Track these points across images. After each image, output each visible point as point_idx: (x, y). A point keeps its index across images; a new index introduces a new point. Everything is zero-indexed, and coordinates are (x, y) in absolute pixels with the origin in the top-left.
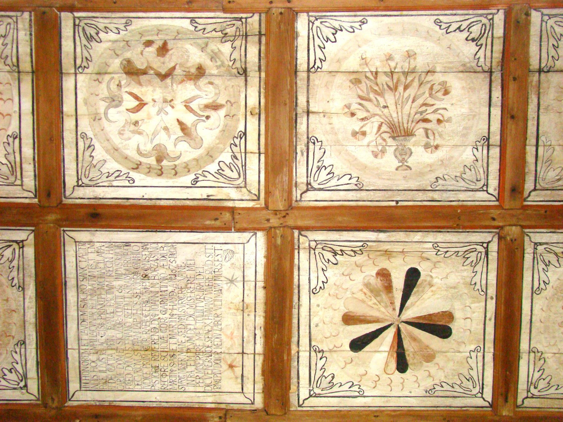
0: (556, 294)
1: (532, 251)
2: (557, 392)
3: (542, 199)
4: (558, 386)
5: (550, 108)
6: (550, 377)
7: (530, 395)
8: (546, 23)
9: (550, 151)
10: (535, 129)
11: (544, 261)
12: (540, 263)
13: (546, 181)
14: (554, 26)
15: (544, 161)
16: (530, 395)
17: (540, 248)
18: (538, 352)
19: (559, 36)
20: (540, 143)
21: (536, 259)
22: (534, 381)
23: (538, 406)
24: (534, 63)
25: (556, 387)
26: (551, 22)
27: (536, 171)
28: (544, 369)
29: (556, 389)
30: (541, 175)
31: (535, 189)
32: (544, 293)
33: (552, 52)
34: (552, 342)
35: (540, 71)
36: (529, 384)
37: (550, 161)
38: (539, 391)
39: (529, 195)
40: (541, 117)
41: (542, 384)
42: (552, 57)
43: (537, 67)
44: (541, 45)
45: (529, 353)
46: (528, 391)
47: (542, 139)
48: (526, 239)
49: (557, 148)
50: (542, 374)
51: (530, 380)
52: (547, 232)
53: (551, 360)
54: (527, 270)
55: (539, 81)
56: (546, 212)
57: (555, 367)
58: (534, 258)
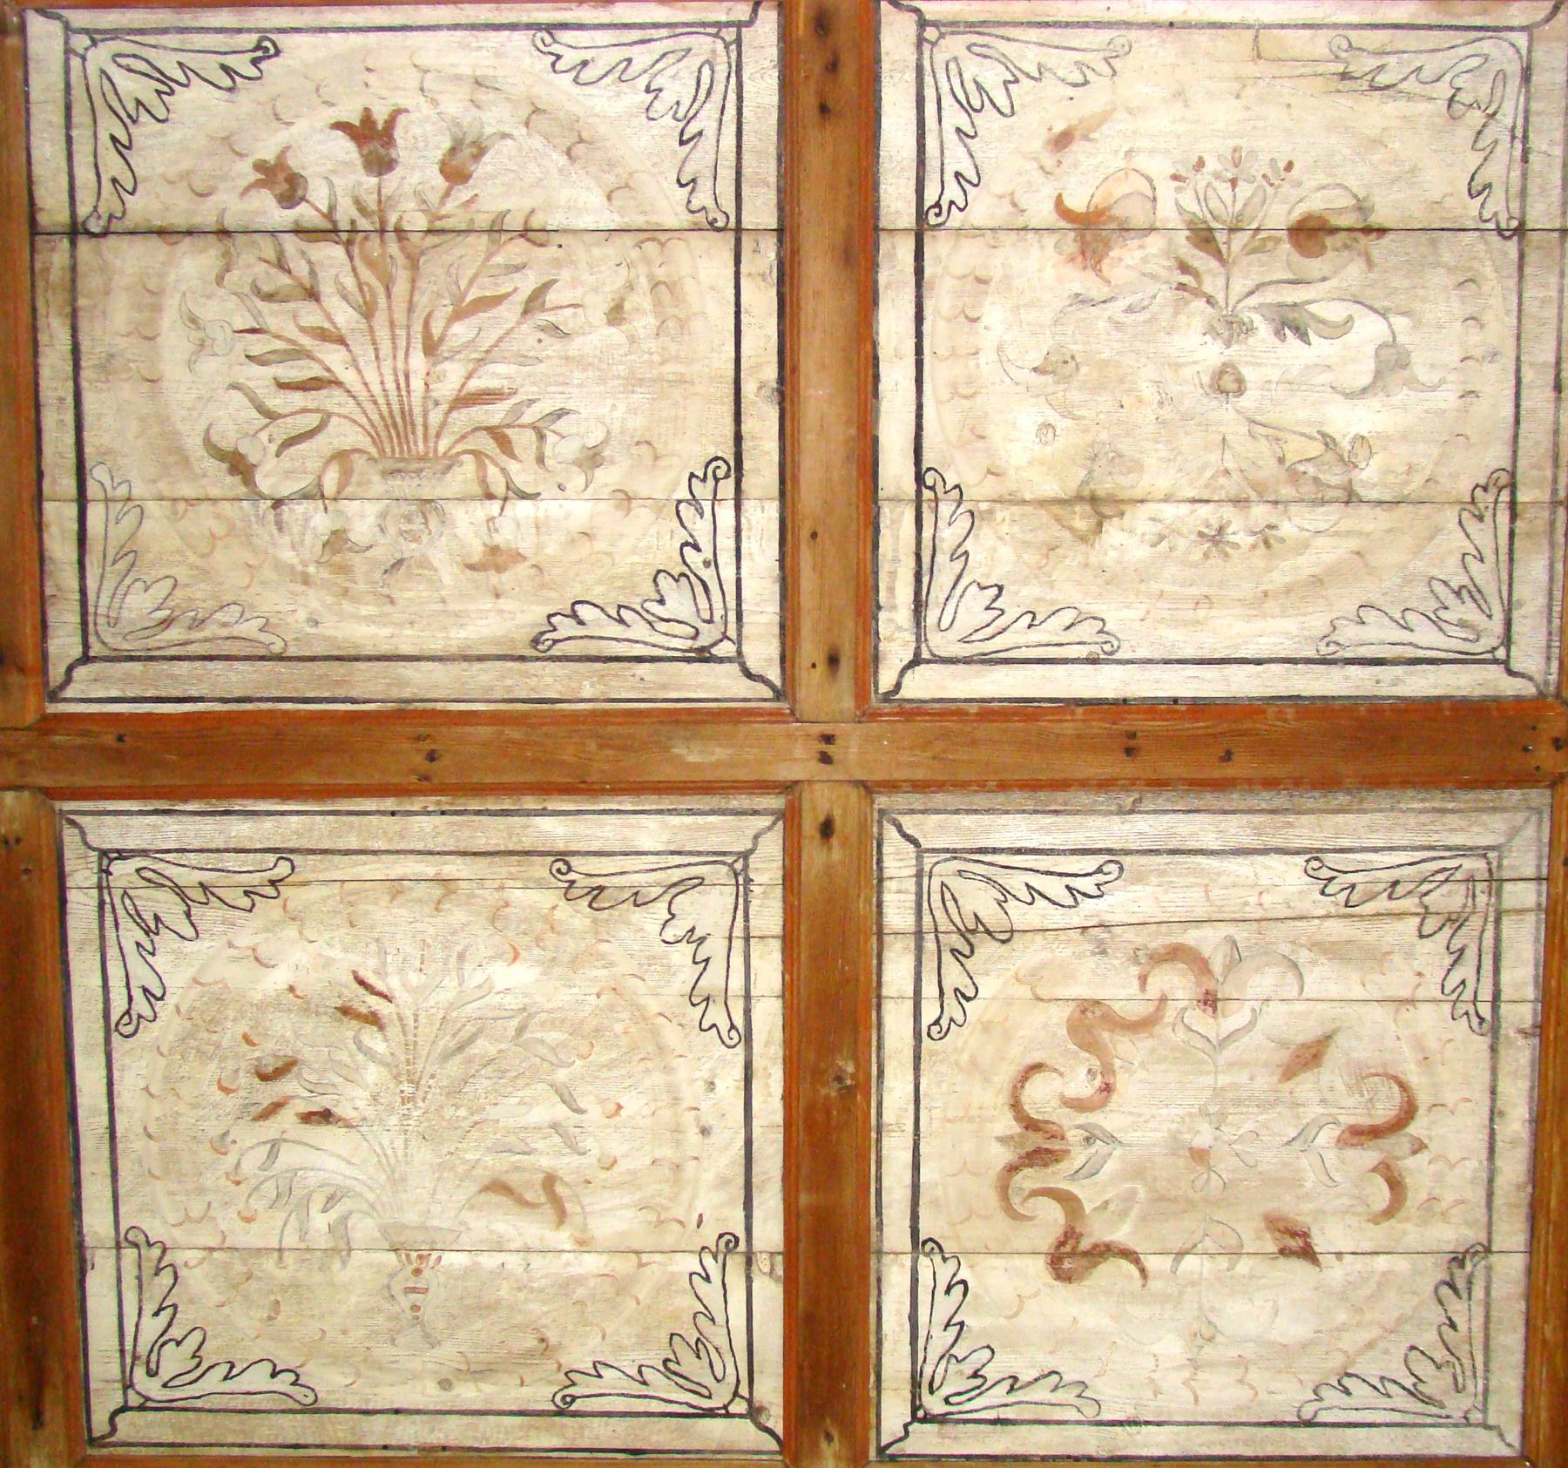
0: (191, 1035)
1: (95, 880)
2: (229, 1386)
3: (114, 693)
4: (232, 1366)
5: (117, 363)
6: (197, 1336)
7: (134, 1400)
8: (84, 59)
9: (129, 521)
10: (70, 439)
11: (137, 917)
12: (126, 922)
13: (124, 627)
14: (113, 71)
15: (110, 559)
16: (134, 1400)
17: (123, 871)
18: (149, 1245)
19: (131, 107)
20: (93, 490)
21: (108, 907)
22: (143, 1350)
23: (169, 1438)
24: (53, 207)
25: (224, 1368)
26: (100, 57)
27: (83, 591)
28: (175, 1306)
29: (226, 1378)
30: (102, 603)
31: (86, 659)
32: (149, 1033)
33: (112, 164)
34: (197, 1209)
35: (75, 231)
36: (129, 1360)
37: (130, 555)
38: (165, 1385)
39: (68, 679)
40: (88, 398)
41: (173, 1361)
42: (114, 181)
43: (63, 217)
44: (69, 140)
45: (118, 1247)
46: (128, 1385)
47: (98, 475)
48: (70, 837)
49: (151, 506)
50: (170, 1325)
51: (129, 1346)
52: (141, 813)
53: (197, 1272)
54: (81, 949)
55: (73, 269)
56: (120, 738)
57: (217, 1298)
58: (101, 904)
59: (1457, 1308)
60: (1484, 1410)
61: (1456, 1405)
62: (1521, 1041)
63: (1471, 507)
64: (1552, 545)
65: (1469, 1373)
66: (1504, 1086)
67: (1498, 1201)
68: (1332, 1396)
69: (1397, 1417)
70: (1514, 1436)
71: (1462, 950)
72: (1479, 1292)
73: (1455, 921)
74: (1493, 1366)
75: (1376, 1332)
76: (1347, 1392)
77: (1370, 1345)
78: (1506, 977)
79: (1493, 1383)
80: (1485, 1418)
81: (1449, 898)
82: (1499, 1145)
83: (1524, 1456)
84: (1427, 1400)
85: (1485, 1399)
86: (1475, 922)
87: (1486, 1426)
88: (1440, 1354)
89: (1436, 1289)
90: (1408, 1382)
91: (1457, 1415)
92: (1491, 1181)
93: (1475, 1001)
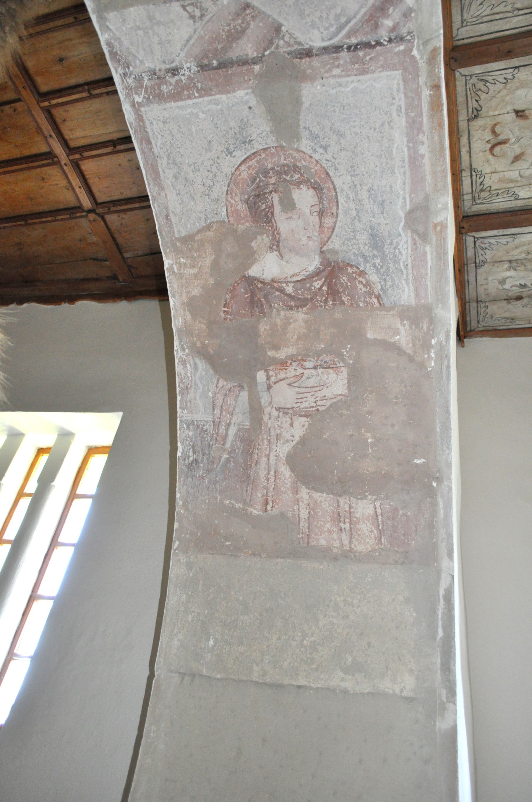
59: (475, 105)
60: (466, 80)
61: (474, 80)
62: (464, 168)
63: (484, 262)
64: (467, 258)
65: (471, 89)
66: (468, 158)
67: (467, 132)
68: (510, 76)
69: (490, 74)
70: (457, 74)
71: (480, 185)
72: (470, 110)
73: (482, 190)
74: (465, 92)
75: (497, 96)
76: (505, 78)
77: (499, 92)
78: (470, 181)
79: (465, 87)
80: (466, 78)
81: (483, 194)
82: (468, 145)
83: (454, 70)
84: (482, 80)
85: (466, 83)
86: (478, 190)
87: (466, 76)
88: (479, 93)
89: (482, 108)
90: (488, 84)
91: (474, 77)
92: (469, 136)
93: (476, 175)
